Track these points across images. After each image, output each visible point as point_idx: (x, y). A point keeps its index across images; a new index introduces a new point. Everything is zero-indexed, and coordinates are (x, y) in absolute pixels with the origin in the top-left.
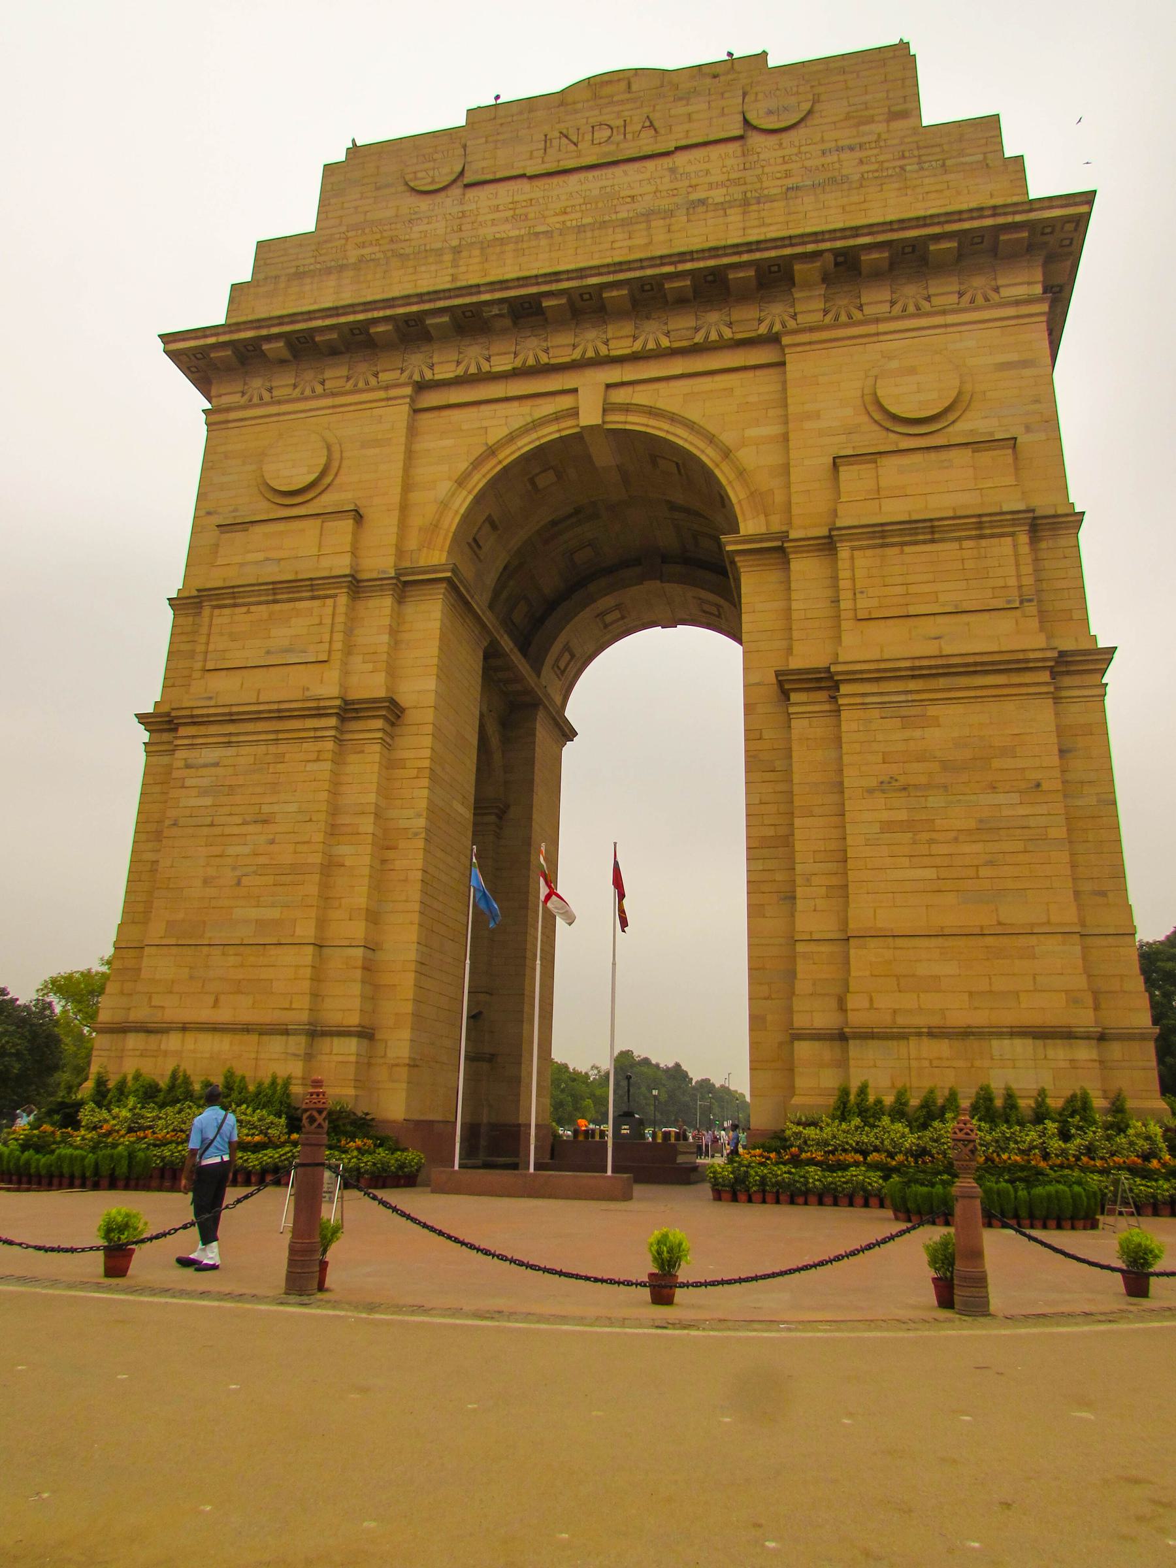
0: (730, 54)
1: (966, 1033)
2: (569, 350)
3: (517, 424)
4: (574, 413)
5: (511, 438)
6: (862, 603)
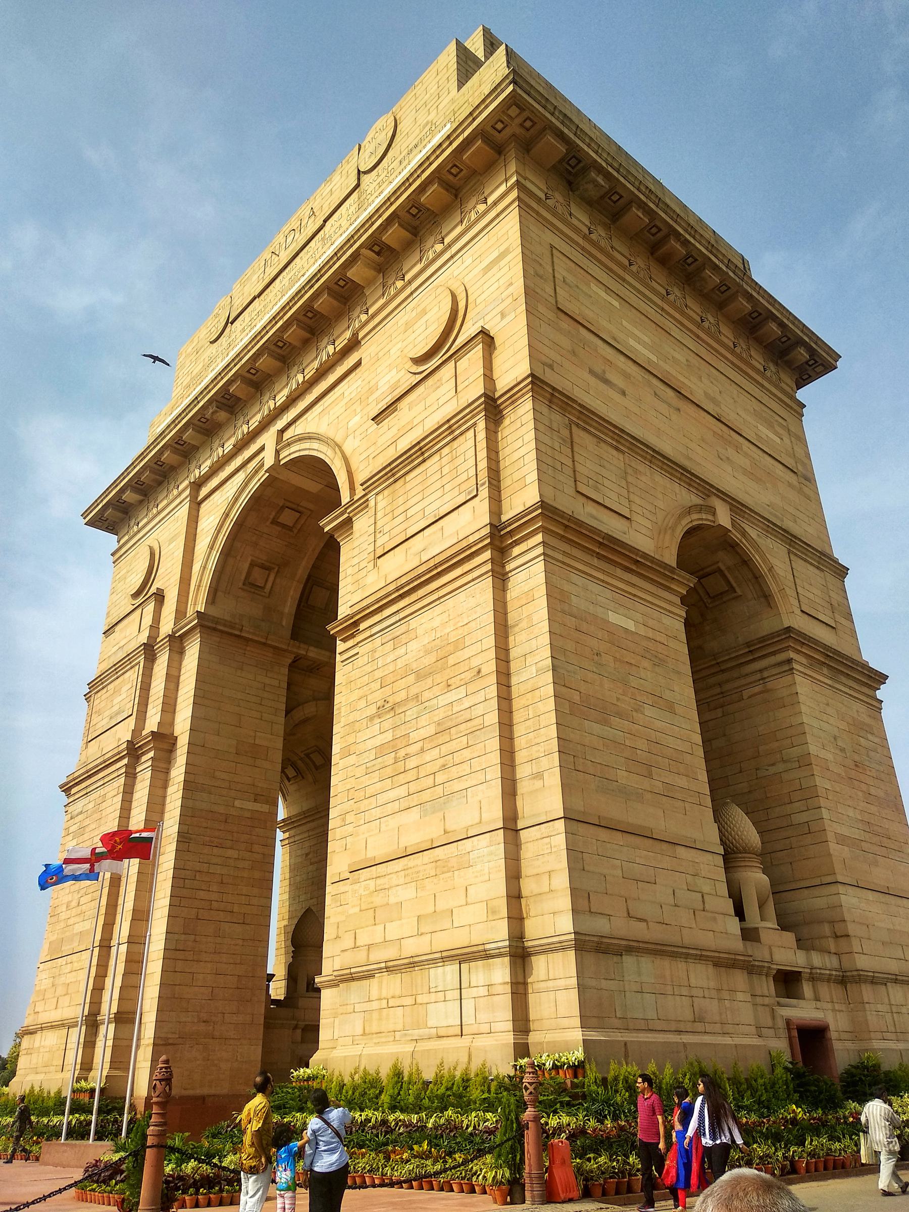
1: (413, 964)
5: (236, 499)
6: (379, 543)
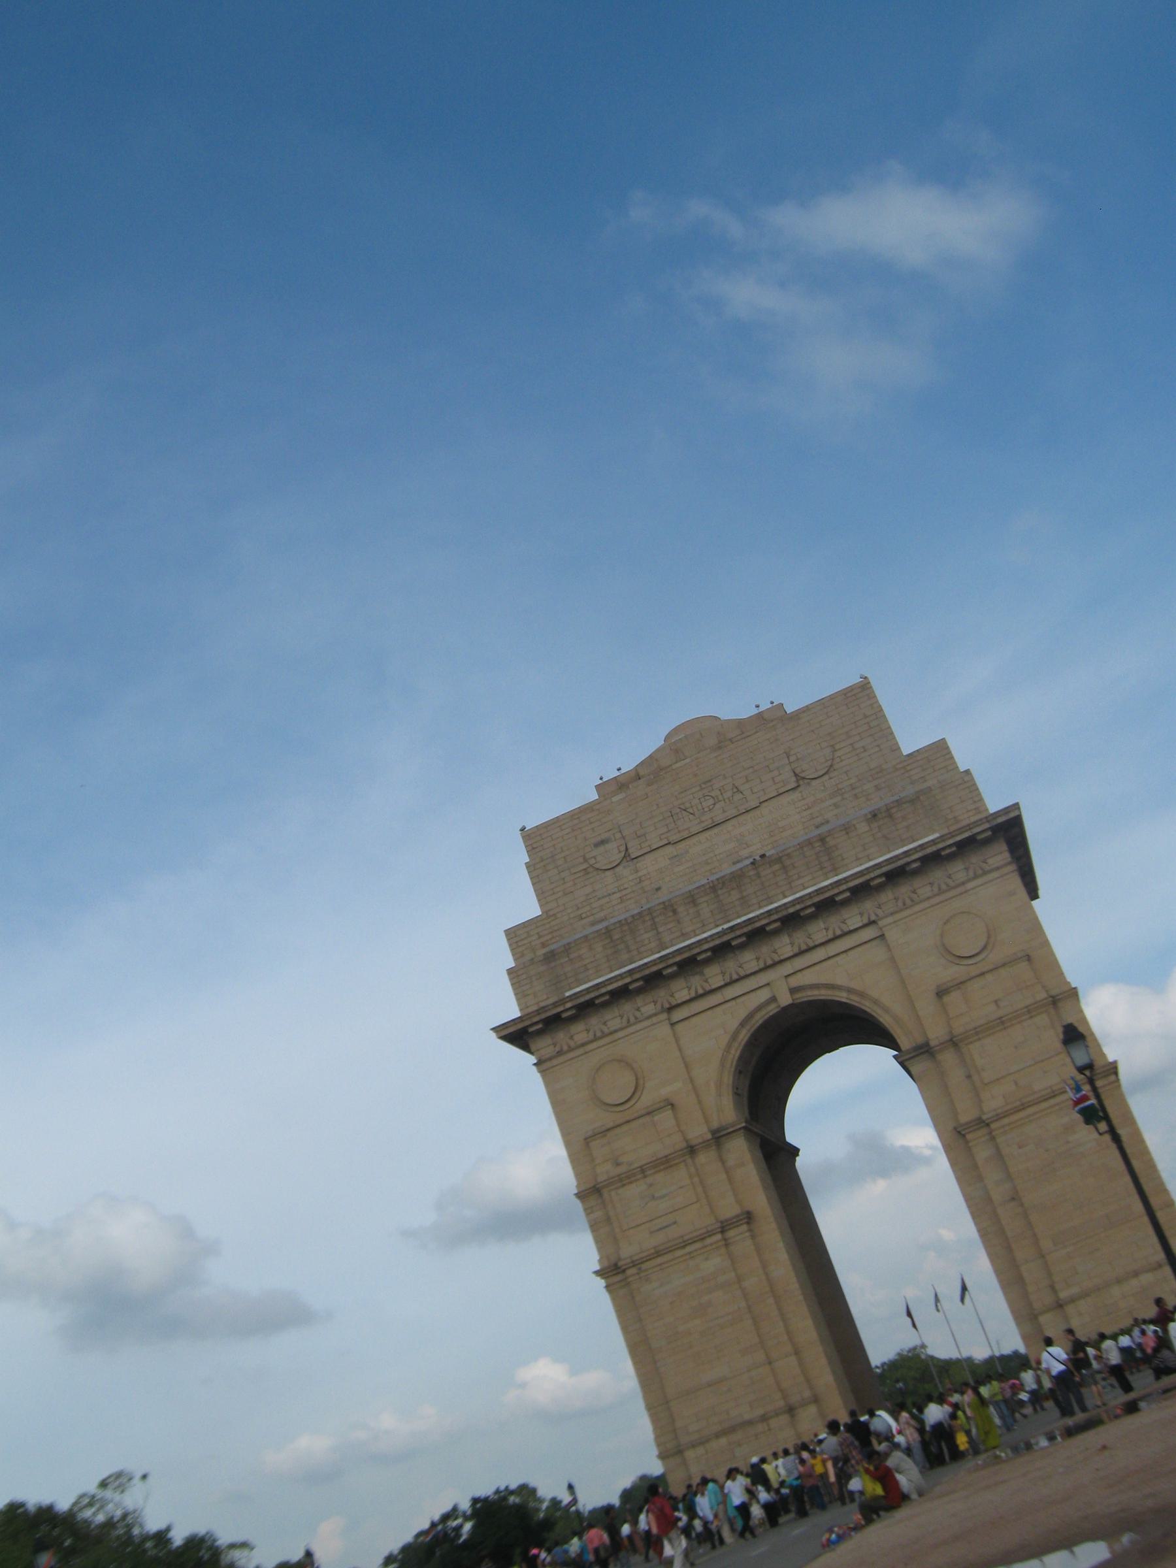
0: (757, 706)
2: (754, 963)
3: (743, 1014)
4: (773, 999)
